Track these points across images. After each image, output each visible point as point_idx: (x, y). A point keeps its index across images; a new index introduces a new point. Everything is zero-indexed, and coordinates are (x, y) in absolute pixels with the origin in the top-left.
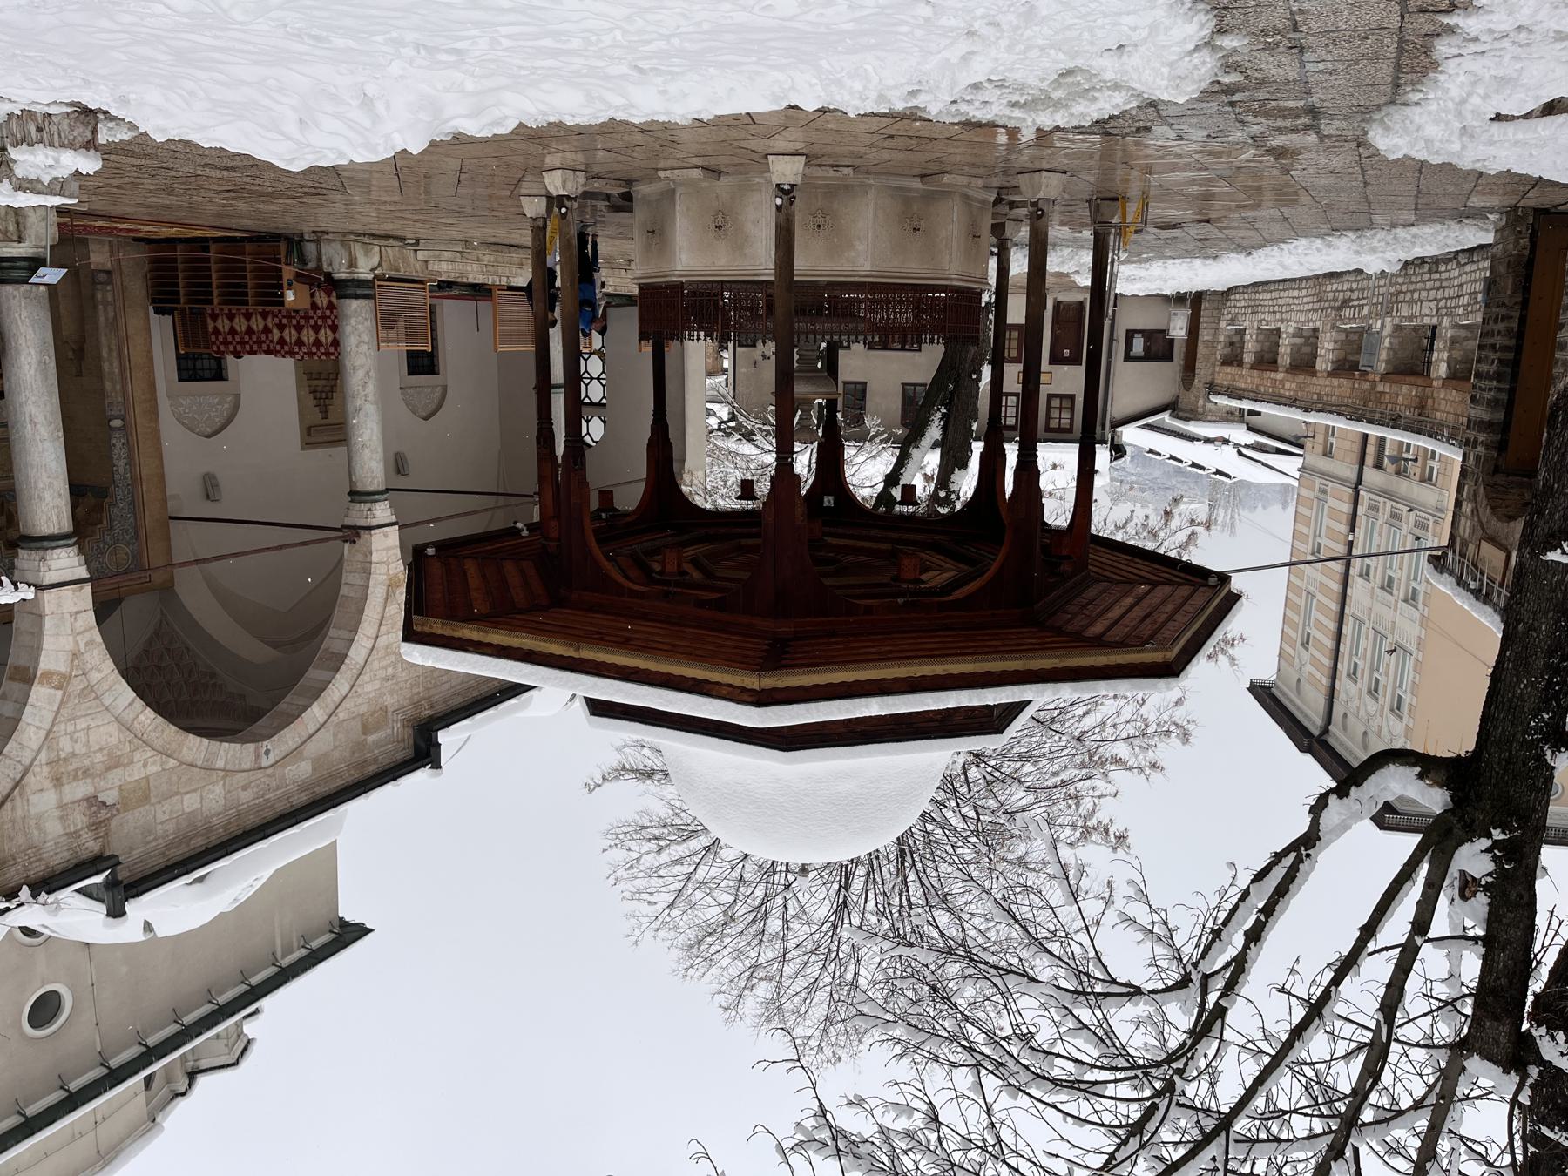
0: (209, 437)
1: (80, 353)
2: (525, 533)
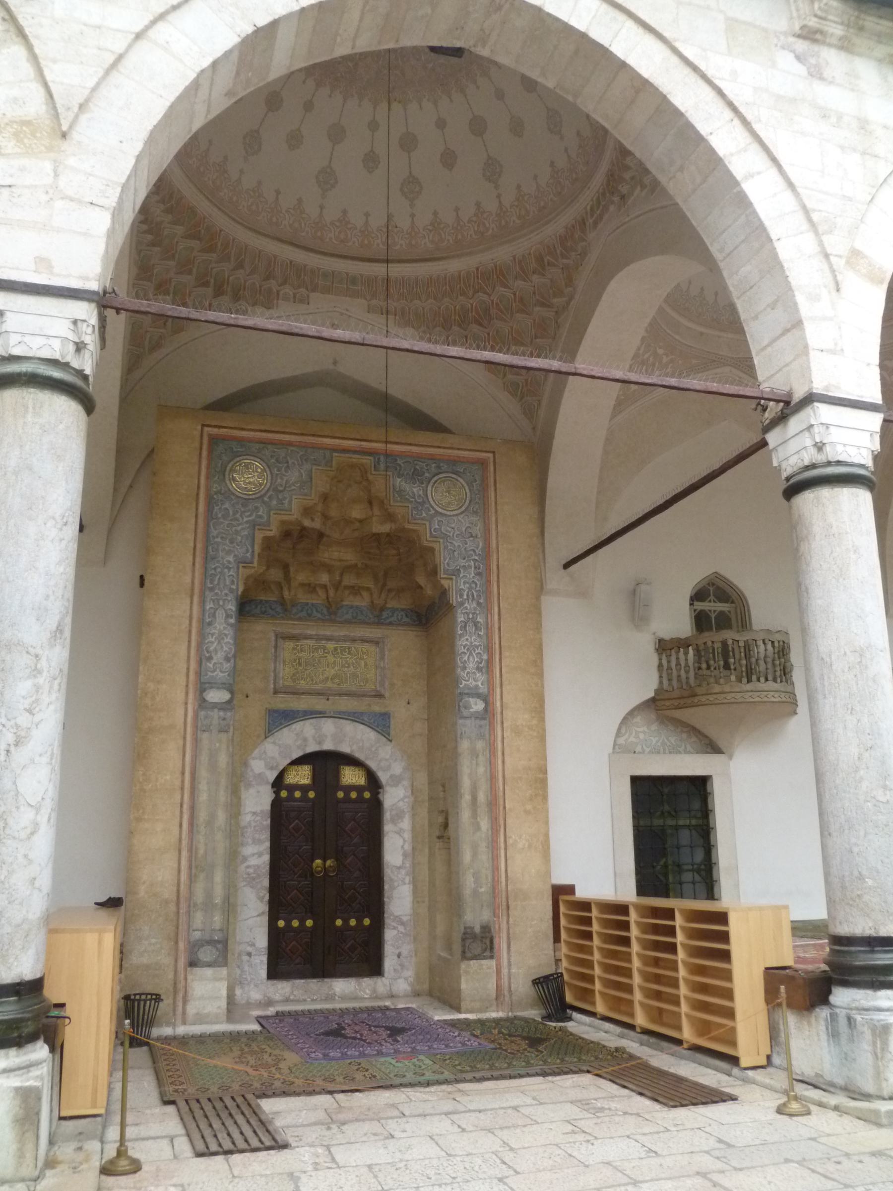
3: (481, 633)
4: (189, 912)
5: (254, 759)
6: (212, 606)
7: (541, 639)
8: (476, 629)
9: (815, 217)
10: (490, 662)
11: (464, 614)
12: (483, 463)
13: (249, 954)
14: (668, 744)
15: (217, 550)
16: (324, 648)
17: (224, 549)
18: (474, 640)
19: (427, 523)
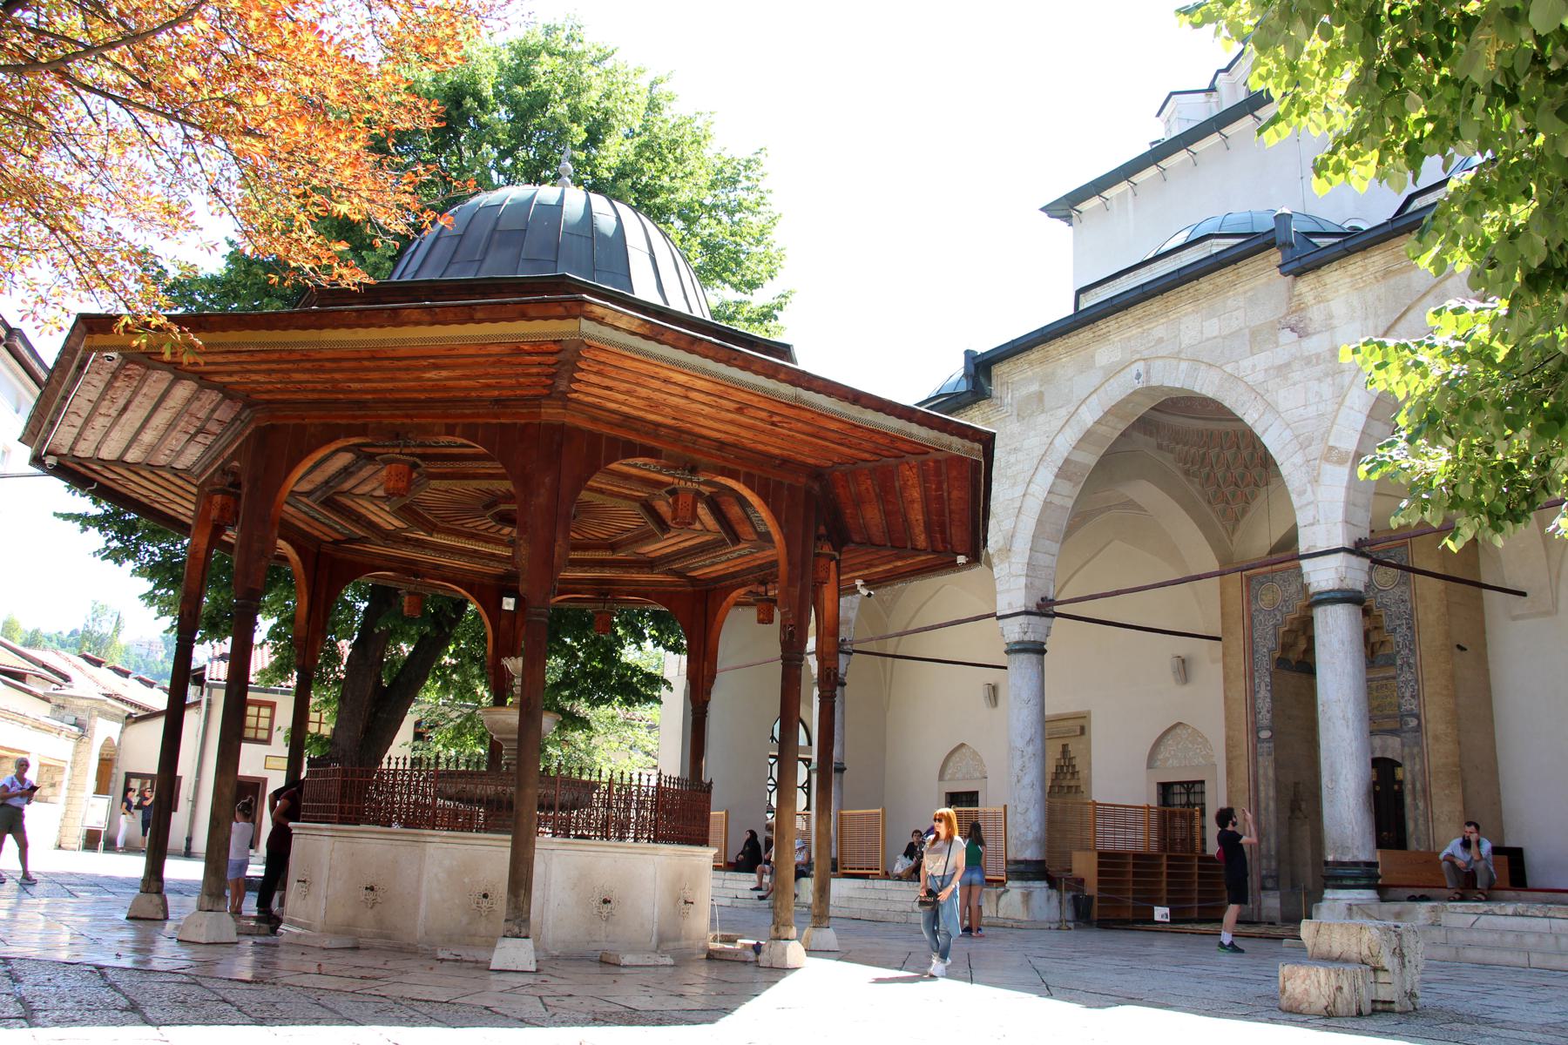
1: (1295, 806)
2: (859, 583)
18: (1409, 676)
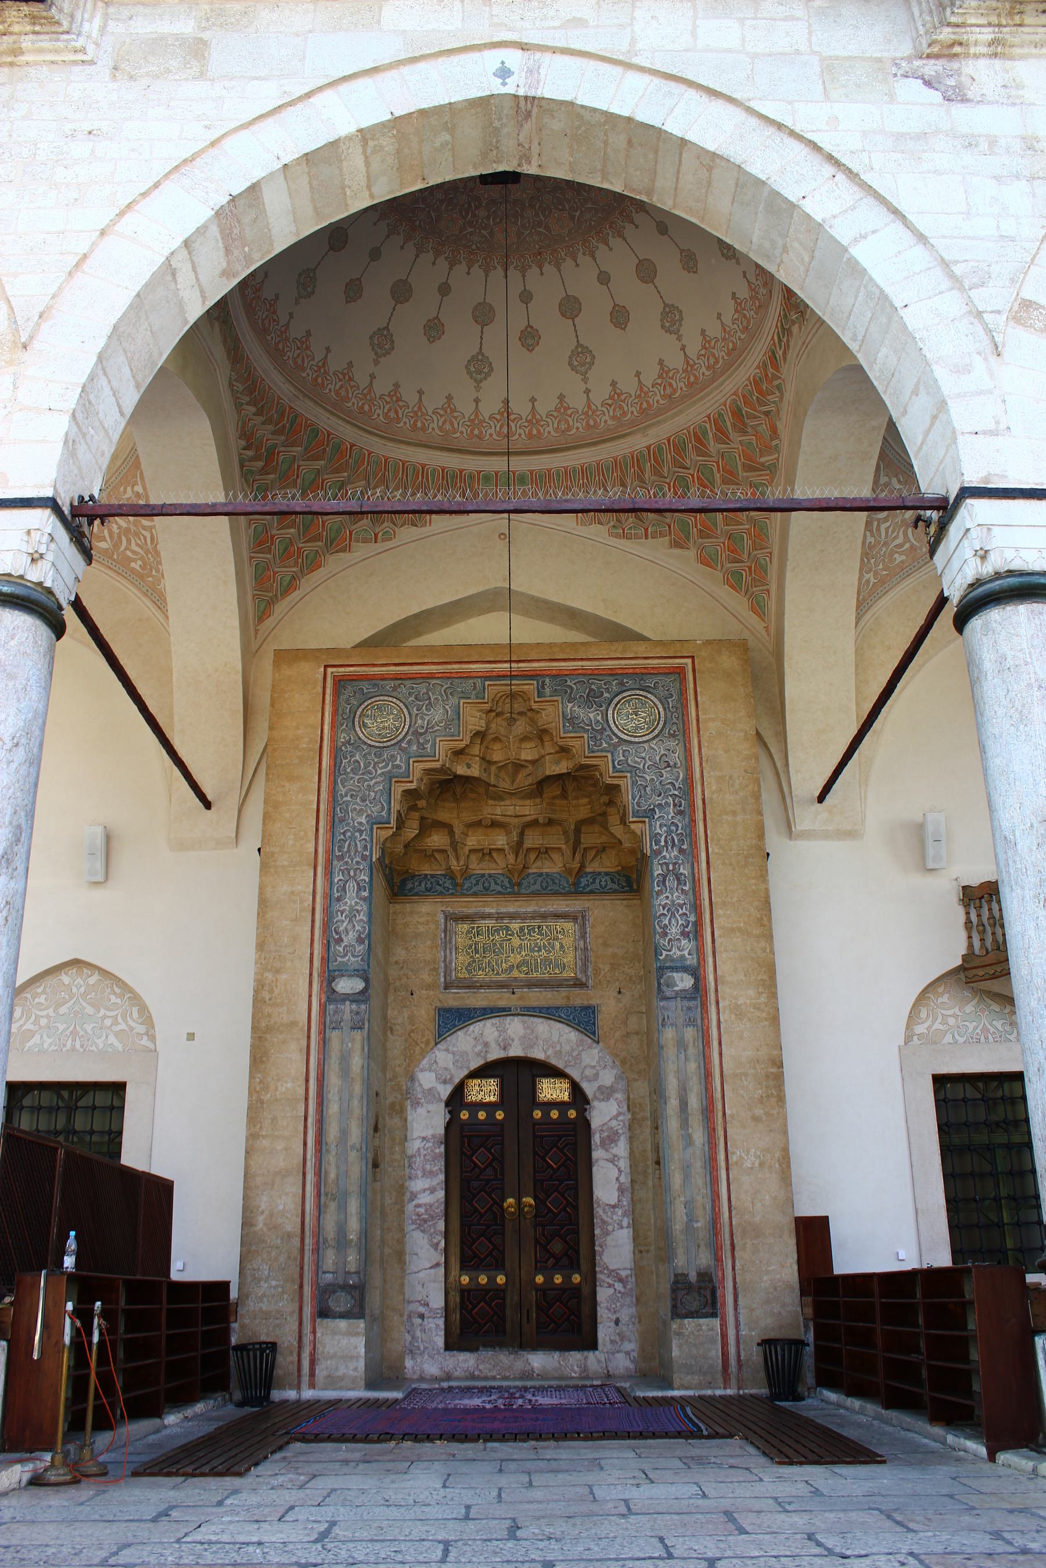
0: (76, 963)
3: (686, 888)
4: (318, 1249)
5: (422, 1071)
6: (341, 877)
7: (767, 889)
8: (679, 883)
9: (958, 270)
10: (698, 924)
11: (661, 865)
12: (680, 672)
13: (422, 1316)
14: (992, 1030)
15: (347, 811)
16: (507, 929)
17: (355, 809)
18: (678, 898)
19: (609, 755)
